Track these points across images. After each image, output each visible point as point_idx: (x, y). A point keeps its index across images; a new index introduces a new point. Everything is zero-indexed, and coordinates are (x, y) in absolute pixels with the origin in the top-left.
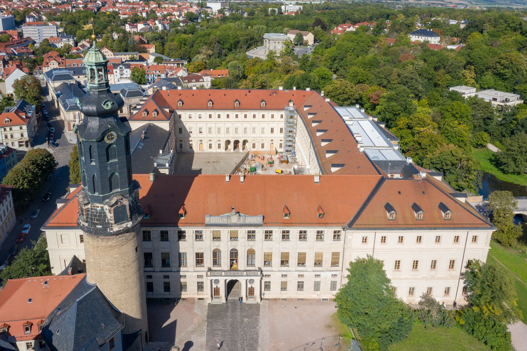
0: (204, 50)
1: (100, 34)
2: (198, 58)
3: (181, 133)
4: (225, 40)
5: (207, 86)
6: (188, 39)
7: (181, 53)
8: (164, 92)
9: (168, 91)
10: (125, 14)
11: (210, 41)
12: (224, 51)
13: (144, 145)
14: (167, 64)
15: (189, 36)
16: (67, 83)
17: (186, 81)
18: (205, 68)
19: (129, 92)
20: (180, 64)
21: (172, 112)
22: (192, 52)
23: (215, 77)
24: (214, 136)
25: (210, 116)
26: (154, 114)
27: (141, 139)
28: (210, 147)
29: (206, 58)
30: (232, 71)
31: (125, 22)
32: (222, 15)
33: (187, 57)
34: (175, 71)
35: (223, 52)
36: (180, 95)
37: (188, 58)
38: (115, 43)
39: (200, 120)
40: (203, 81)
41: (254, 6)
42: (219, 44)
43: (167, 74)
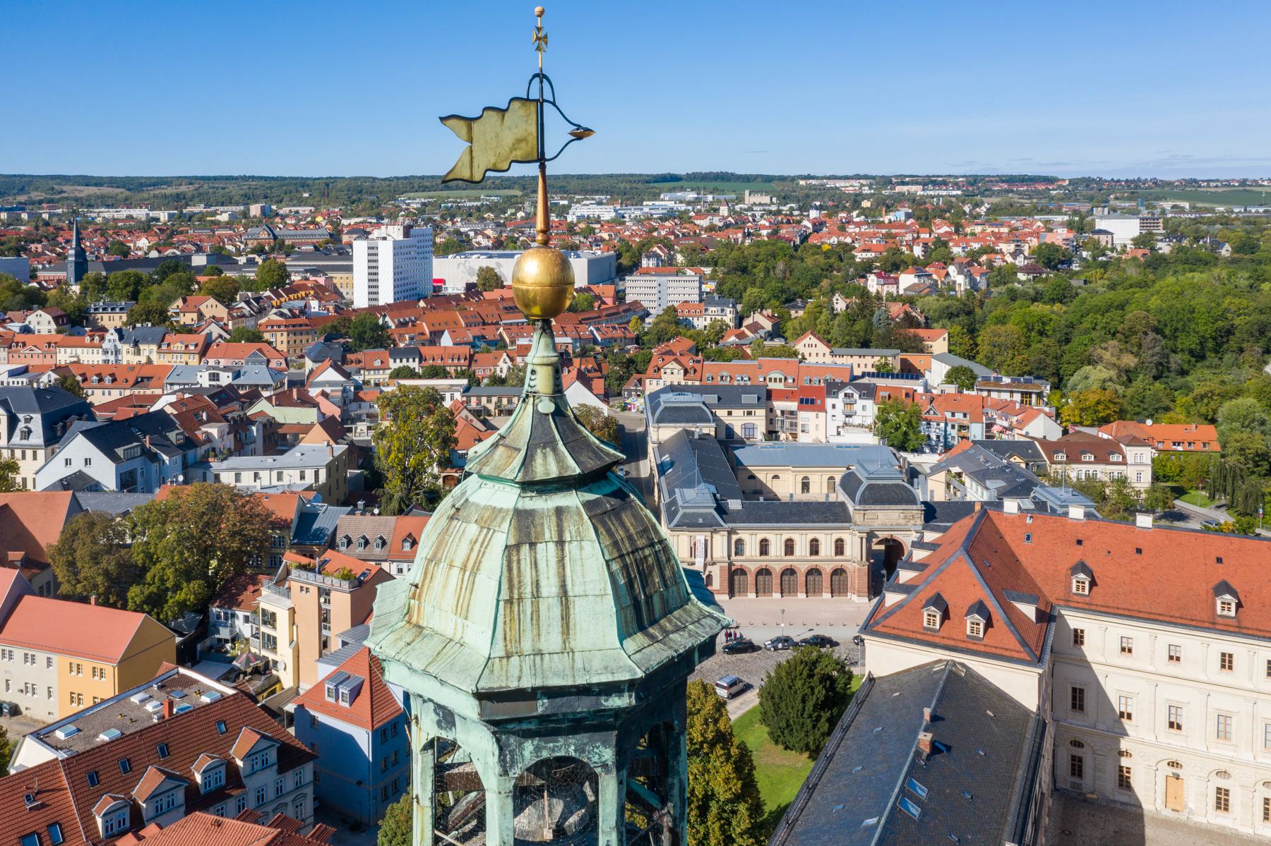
0: (1109, 351)
1: (801, 297)
2: (1086, 378)
3: (1081, 708)
4: (1180, 326)
5: (1139, 479)
6: (1053, 316)
7: (1032, 359)
8: (1010, 519)
9: (1029, 521)
10: (868, 251)
11: (1127, 325)
12: (1176, 360)
13: (930, 798)
14: (989, 391)
15: (1055, 308)
16: (693, 432)
17: (1061, 457)
18: (1122, 414)
19: (870, 487)
20: (1031, 394)
21: (1047, 616)
22: (1066, 357)
23: (1161, 446)
24: (1246, 756)
25: (1227, 662)
26: (972, 624)
27: (918, 753)
28: (1222, 800)
29: (1115, 378)
30: (1237, 436)
31: (867, 268)
32: (1148, 251)
33: (1051, 370)
34: (1020, 417)
35: (1172, 360)
36: (1079, 542)
37: (1053, 374)
38: (836, 322)
39: (1173, 668)
40: (1124, 463)
41: (1249, 227)
42: (1159, 337)
43: (989, 426)
